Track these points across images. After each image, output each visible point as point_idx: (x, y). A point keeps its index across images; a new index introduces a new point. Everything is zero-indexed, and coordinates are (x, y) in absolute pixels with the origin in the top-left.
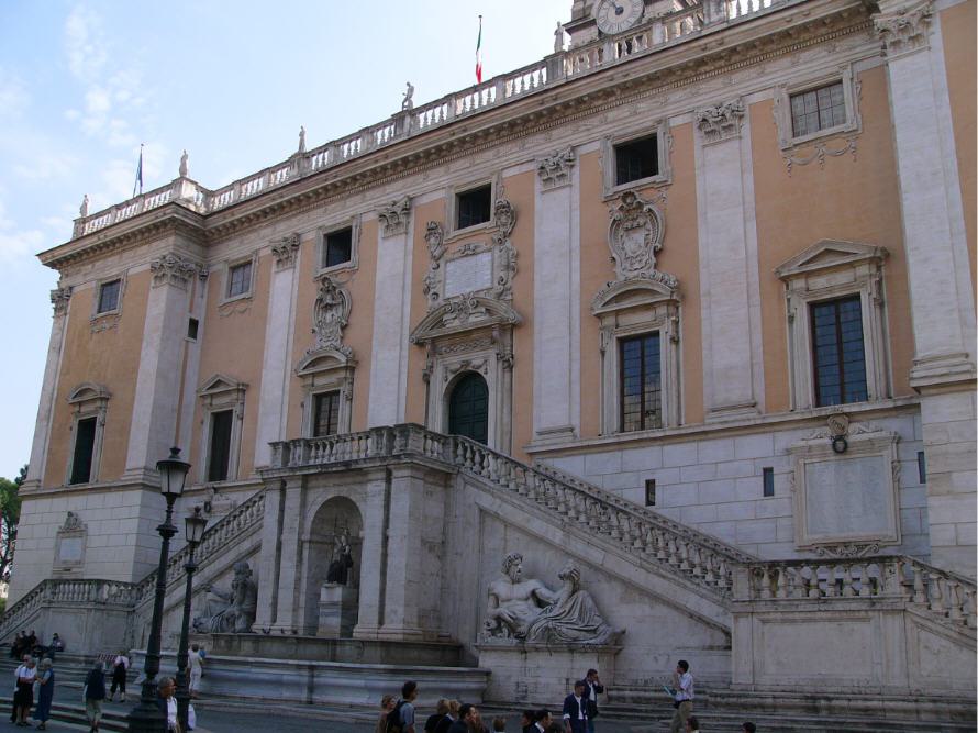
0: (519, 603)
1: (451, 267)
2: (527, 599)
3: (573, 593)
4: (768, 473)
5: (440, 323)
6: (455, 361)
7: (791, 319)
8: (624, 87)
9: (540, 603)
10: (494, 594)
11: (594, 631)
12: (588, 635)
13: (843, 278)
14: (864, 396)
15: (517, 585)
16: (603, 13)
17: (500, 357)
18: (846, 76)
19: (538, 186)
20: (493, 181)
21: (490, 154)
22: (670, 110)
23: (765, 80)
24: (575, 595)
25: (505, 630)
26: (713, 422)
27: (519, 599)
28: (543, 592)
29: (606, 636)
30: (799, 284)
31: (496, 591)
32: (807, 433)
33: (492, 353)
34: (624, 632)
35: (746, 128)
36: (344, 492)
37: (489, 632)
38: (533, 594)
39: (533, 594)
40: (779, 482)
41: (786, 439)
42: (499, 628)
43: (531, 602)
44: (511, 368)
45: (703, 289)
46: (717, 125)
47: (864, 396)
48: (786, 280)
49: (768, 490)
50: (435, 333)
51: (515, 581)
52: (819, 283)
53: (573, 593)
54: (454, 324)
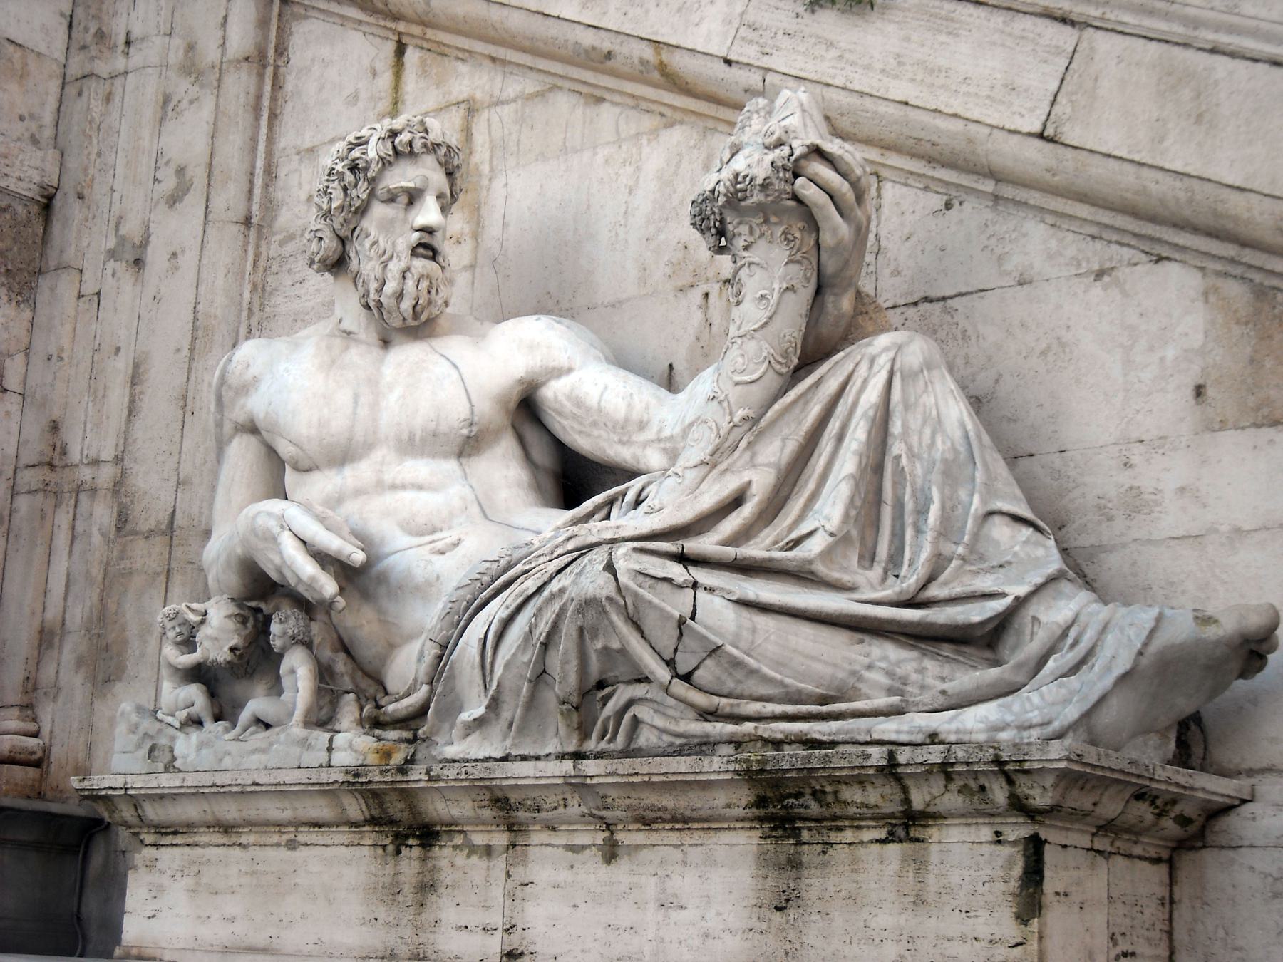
0: (419, 468)
2: (470, 445)
3: (812, 354)
9: (574, 478)
10: (252, 428)
11: (987, 639)
12: (933, 673)
15: (408, 354)
24: (830, 375)
25: (298, 672)
27: (420, 443)
28: (598, 397)
29: (1096, 680)
31: (256, 405)
34: (1252, 651)
37: (195, 694)
38: (527, 408)
39: (527, 408)
42: (257, 658)
43: (504, 471)
51: (408, 323)
53: (812, 354)
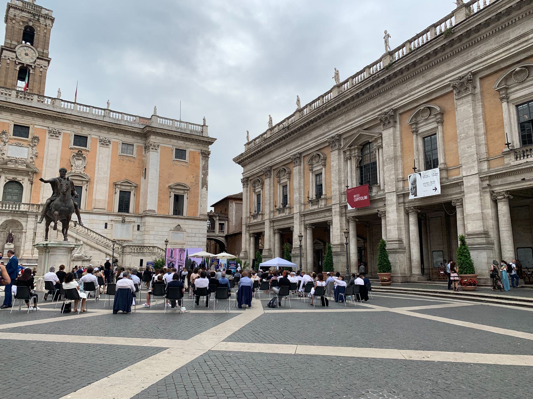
1: (11, 147)
4: (106, 224)
5: (6, 164)
6: (11, 177)
7: (116, 193)
8: (83, 122)
13: (128, 188)
14: (128, 212)
16: (19, 51)
17: (29, 180)
18: (135, 145)
19: (47, 135)
20: (31, 126)
21: (30, 118)
22: (92, 133)
23: (117, 137)
26: (95, 211)
30: (119, 186)
32: (117, 217)
33: (26, 179)
35: (111, 146)
36: (16, 218)
40: (108, 226)
41: (111, 218)
44: (32, 184)
45: (95, 180)
46: (105, 143)
47: (128, 212)
48: (116, 185)
49: (106, 227)
50: (4, 166)
52: (123, 187)
54: (11, 166)
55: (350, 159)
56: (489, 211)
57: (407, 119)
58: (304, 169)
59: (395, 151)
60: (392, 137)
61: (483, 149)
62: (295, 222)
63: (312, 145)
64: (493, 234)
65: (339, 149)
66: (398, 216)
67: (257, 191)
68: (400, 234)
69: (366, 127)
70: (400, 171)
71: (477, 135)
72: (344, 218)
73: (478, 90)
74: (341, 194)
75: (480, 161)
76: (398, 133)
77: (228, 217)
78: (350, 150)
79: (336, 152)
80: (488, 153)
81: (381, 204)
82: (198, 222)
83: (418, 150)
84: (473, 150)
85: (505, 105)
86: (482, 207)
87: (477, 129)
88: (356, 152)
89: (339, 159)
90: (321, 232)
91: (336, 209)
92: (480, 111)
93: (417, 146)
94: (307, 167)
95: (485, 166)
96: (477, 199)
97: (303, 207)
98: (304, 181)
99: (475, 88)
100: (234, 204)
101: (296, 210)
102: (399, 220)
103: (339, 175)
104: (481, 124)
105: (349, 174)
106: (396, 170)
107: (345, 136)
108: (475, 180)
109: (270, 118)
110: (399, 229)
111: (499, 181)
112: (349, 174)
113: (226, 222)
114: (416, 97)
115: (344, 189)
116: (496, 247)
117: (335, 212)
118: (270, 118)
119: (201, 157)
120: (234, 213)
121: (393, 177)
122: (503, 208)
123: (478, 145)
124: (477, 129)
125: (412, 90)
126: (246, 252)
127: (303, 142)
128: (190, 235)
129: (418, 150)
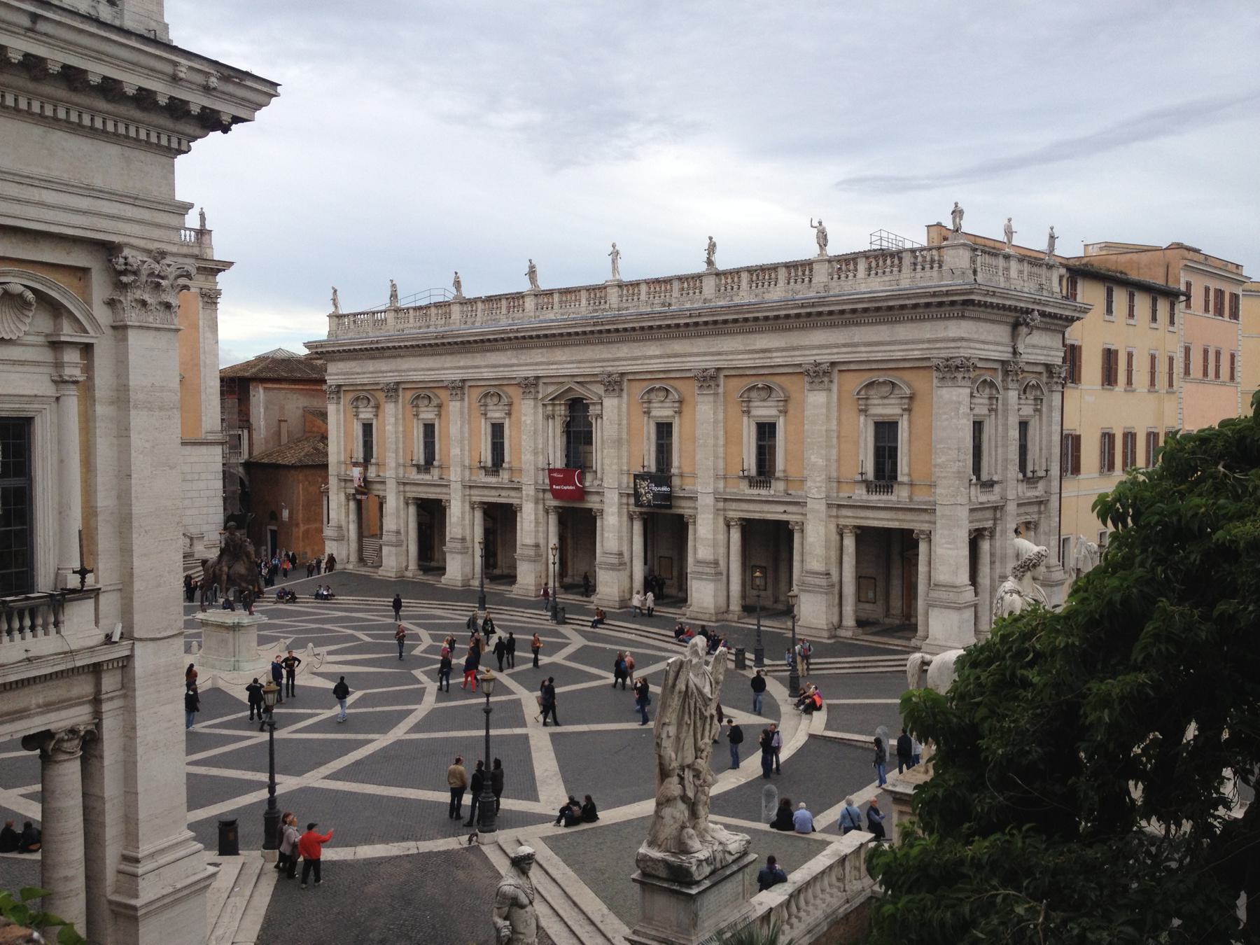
55: (553, 417)
56: (721, 537)
57: (638, 389)
58: (469, 408)
59: (620, 432)
60: (616, 411)
61: (721, 464)
62: (453, 495)
63: (486, 375)
64: (722, 563)
65: (535, 399)
66: (620, 522)
67: (361, 416)
68: (620, 545)
69: (579, 380)
70: (625, 460)
71: (715, 446)
72: (541, 507)
73: (721, 390)
74: (537, 469)
75: (717, 477)
76: (625, 406)
77: (248, 421)
78: (554, 405)
79: (532, 402)
80: (725, 469)
81: (595, 498)
82: (204, 449)
83: (648, 439)
84: (710, 464)
85: (745, 419)
86: (715, 532)
87: (716, 438)
88: (561, 410)
89: (535, 413)
90: (499, 520)
91: (529, 491)
92: (721, 417)
93: (649, 433)
94: (476, 405)
95: (721, 484)
96: (711, 522)
97: (467, 473)
98: (470, 430)
99: (718, 386)
100: (261, 391)
101: (455, 475)
102: (621, 526)
103: (535, 440)
104: (721, 433)
105: (551, 442)
106: (620, 457)
107: (545, 380)
108: (710, 500)
109: (394, 286)
110: (620, 538)
111: (734, 506)
112: (551, 442)
113: (246, 432)
114: (650, 368)
115: (541, 462)
116: (724, 578)
117: (528, 495)
118: (394, 286)
119: (201, 304)
120: (262, 410)
121: (615, 467)
122: (736, 535)
123: (716, 457)
124: (716, 438)
125: (646, 357)
126: (340, 527)
127: (470, 363)
128: (189, 477)
129: (648, 439)
